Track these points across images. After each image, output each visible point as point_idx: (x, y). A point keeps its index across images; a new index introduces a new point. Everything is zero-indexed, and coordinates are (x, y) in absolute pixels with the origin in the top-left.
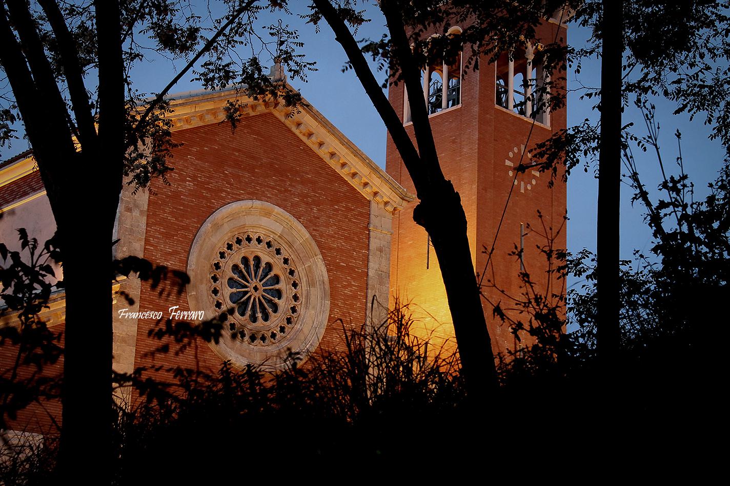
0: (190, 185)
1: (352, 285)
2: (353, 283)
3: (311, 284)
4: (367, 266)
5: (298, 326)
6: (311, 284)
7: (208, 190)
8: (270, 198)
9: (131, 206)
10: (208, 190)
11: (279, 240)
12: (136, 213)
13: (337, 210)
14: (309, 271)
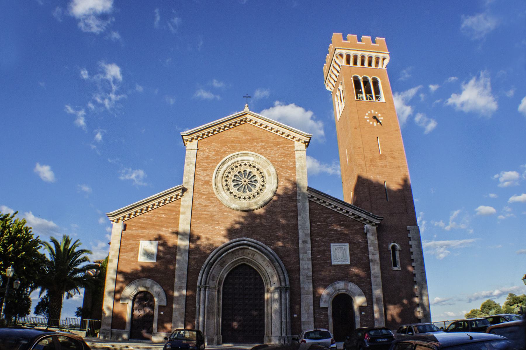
0: (213, 153)
1: (288, 172)
3: (270, 175)
4: (295, 164)
5: (265, 191)
6: (270, 175)
7: (221, 153)
8: (248, 150)
9: (189, 163)
10: (221, 153)
11: (254, 163)
12: (191, 165)
13: (279, 148)
14: (268, 171)
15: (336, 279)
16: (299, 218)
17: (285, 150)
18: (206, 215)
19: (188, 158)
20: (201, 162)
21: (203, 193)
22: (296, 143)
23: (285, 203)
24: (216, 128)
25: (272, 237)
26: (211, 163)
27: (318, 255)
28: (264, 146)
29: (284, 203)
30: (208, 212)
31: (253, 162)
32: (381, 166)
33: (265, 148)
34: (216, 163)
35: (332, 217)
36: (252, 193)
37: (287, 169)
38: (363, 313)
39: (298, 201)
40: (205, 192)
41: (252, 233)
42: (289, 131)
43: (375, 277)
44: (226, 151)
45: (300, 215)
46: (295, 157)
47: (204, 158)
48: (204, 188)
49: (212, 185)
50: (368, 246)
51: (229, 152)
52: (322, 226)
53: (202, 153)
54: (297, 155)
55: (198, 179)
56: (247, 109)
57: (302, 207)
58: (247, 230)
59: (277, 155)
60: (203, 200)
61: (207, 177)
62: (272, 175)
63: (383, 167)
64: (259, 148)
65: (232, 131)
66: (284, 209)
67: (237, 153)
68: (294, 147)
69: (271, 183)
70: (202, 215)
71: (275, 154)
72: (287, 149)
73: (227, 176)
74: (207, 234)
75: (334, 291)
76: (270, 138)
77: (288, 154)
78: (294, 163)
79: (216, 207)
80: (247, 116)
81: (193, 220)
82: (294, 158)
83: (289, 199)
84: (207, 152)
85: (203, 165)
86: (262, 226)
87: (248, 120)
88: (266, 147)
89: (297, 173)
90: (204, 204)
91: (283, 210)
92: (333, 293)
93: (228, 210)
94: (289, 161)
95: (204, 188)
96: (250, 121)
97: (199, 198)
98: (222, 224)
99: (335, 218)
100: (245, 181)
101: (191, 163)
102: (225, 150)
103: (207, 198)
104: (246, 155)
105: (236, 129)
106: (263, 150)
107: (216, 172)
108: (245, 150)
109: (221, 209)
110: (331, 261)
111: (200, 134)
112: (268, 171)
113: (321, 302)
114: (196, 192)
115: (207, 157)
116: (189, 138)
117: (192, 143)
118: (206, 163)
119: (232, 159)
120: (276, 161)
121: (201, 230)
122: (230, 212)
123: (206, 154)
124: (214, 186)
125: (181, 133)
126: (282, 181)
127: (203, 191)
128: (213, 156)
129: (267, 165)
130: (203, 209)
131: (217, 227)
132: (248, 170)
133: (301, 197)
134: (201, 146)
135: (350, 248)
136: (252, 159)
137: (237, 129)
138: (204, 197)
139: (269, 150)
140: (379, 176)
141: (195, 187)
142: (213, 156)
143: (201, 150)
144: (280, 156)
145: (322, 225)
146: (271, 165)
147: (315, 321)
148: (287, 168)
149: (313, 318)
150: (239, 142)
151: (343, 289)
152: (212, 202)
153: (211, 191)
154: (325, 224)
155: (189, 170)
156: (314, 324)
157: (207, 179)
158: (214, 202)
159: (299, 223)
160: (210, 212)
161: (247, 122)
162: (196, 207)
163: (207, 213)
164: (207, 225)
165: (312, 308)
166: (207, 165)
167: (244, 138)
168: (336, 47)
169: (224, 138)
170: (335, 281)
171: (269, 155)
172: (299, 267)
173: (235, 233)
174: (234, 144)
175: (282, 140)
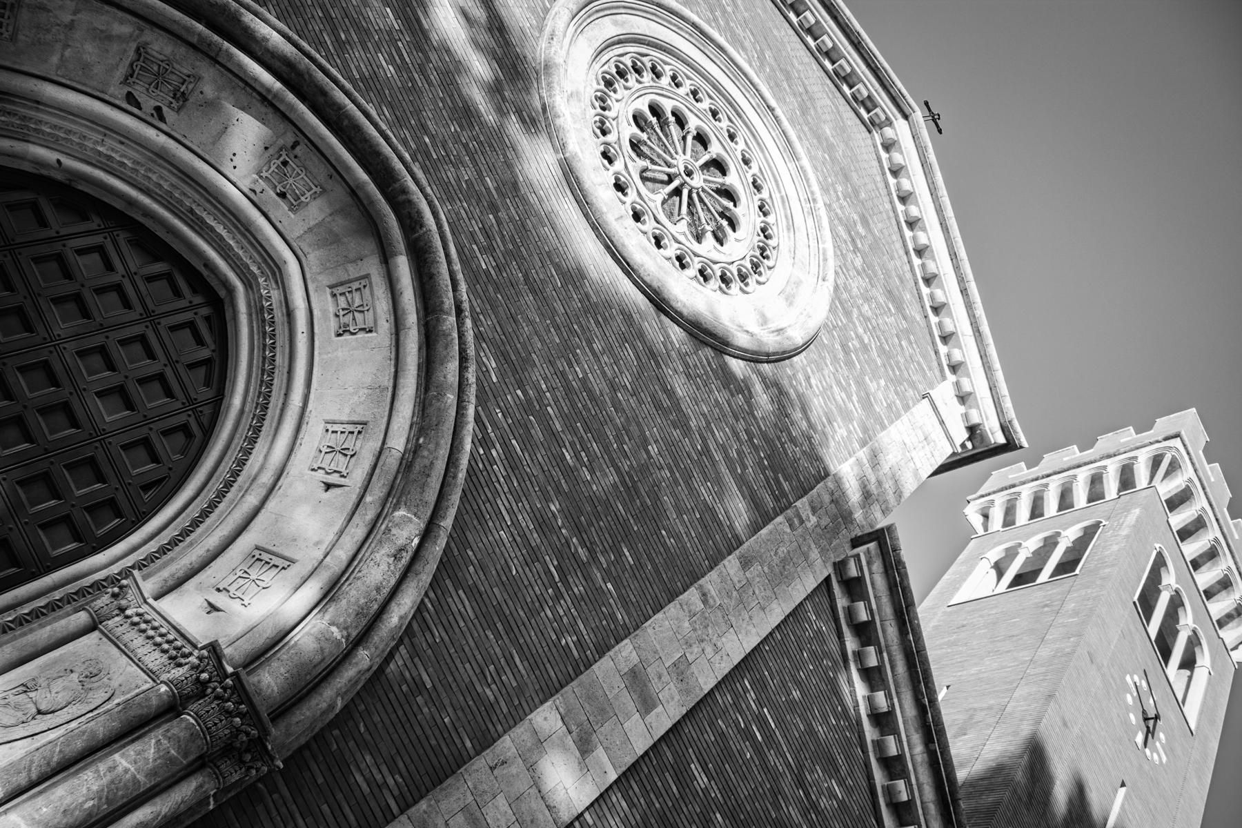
1: (849, 397)
7: (727, 23)
17: (901, 345)
25: (537, 433)
31: (776, 196)
52: (772, 757)
80: (901, 124)
86: (557, 328)
87: (888, 132)
99: (841, 803)
129: (814, 269)
133: (814, 519)
154: (789, 766)
159: (710, 581)
168: (1183, 433)
172: (461, 760)
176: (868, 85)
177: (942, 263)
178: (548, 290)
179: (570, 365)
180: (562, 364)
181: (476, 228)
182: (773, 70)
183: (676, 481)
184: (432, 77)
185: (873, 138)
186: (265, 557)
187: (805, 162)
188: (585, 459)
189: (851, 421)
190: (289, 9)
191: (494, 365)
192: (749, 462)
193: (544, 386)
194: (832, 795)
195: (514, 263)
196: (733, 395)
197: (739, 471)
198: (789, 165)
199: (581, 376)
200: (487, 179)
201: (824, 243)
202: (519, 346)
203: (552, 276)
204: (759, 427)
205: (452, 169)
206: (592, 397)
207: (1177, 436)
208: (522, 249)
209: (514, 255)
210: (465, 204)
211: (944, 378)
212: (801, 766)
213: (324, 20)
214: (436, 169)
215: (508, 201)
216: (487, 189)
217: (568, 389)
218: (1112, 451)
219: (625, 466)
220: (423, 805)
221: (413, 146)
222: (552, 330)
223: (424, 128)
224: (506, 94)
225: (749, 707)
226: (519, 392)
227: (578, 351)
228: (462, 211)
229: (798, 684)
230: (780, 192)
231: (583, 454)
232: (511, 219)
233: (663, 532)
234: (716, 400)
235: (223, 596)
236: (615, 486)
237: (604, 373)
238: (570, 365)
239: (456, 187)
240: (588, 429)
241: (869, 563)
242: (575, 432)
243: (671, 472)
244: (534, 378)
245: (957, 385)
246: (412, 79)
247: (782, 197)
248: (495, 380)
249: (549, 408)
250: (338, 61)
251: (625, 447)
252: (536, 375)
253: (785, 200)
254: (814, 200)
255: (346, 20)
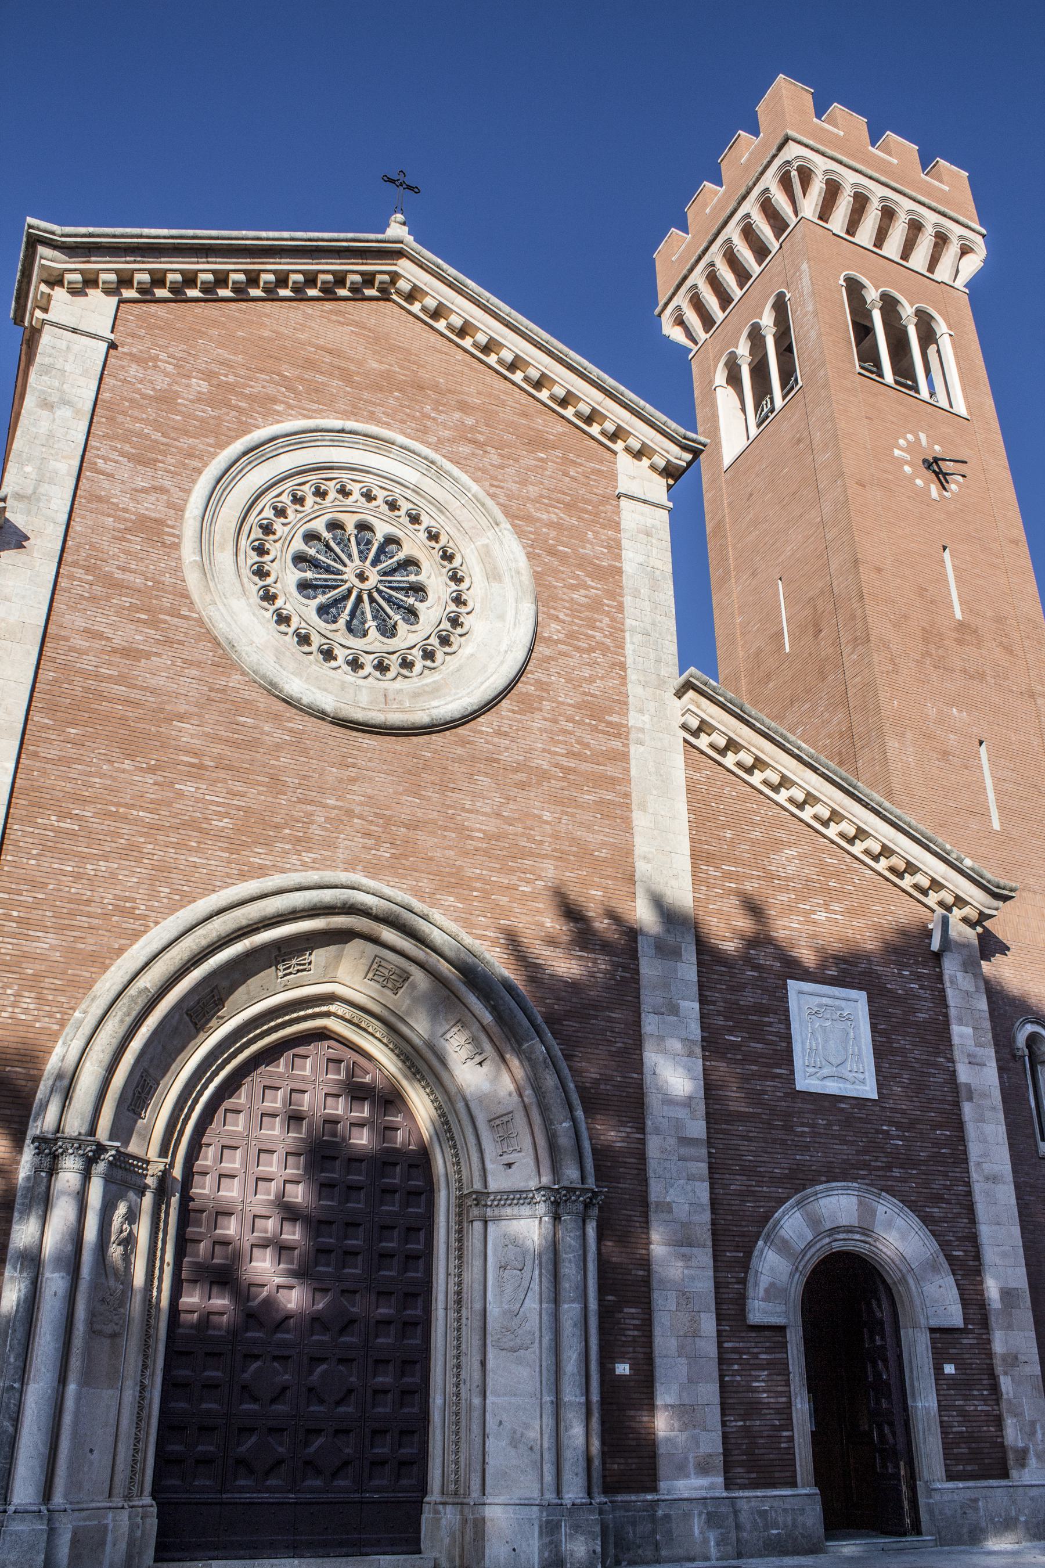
1: (587, 587)
2: (590, 583)
3: (493, 575)
4: (619, 557)
6: (493, 575)
7: (246, 397)
9: (54, 399)
10: (246, 397)
13: (541, 460)
14: (485, 555)
15: (819, 1173)
16: (640, 820)
17: (573, 478)
18: (127, 702)
19: (48, 369)
20: (124, 413)
21: (118, 575)
22: (624, 461)
23: (571, 733)
24: (236, 270)
25: (503, 900)
26: (186, 433)
27: (731, 1031)
28: (473, 429)
29: (564, 731)
30: (144, 689)
31: (409, 494)
32: (964, 671)
33: (474, 442)
34: (211, 441)
35: (790, 845)
36: (394, 643)
37: (580, 566)
38: (949, 1369)
39: (633, 736)
40: (129, 577)
41: (394, 856)
42: (599, 396)
43: (987, 1179)
44: (274, 400)
45: (643, 807)
46: (619, 523)
47: (144, 396)
48: (127, 553)
49: (176, 546)
50: (946, 1016)
51: (290, 407)
53: (134, 371)
54: (630, 515)
55: (99, 499)
56: (397, 230)
57: (652, 770)
58: (368, 835)
59: (533, 491)
60: (118, 614)
61: (152, 498)
62: (507, 579)
63: (972, 677)
64: (447, 433)
65: (310, 311)
66: (564, 762)
67: (338, 424)
68: (613, 476)
69: (501, 617)
70: (101, 696)
71: (524, 482)
72: (581, 478)
73: (267, 529)
74: (124, 818)
75: (810, 1237)
76: (503, 404)
77: (588, 502)
78: (615, 548)
79: (194, 672)
80: (404, 266)
81: (36, 717)
82: (616, 526)
83: (591, 717)
84: (167, 374)
85: (139, 434)
86: (445, 828)
87: (403, 285)
88: (481, 438)
89: (628, 600)
90: (118, 641)
91: (557, 765)
92: (810, 1245)
93: (263, 701)
94: (590, 535)
95: (127, 553)
96: (412, 296)
97: (93, 599)
98: (222, 774)
99: (801, 857)
100: (362, 577)
101: (65, 402)
102: (271, 390)
103: (139, 610)
104: (382, 444)
105: (330, 312)
106: (465, 449)
107: (213, 482)
108: (372, 418)
109: (222, 691)
110: (792, 1072)
111: (142, 270)
112: (485, 555)
113: (750, 1292)
114: (75, 564)
115: (166, 399)
116: (73, 268)
117: (80, 300)
118: (157, 425)
119: (300, 446)
120: (529, 519)
121: (88, 785)
122: (277, 717)
123: (162, 383)
124: (188, 553)
125: (30, 220)
126: (557, 619)
127: (119, 568)
128: (199, 400)
129: (484, 522)
130: (109, 664)
131: (188, 788)
132: (382, 529)
133: (646, 718)
134: (133, 336)
135: (872, 1015)
136: (409, 475)
137: (338, 313)
138: (126, 601)
139: (496, 459)
140: (960, 711)
141: (71, 533)
142: (199, 400)
143: (131, 355)
144: (549, 498)
145: (750, 877)
146: (506, 525)
147: (725, 1408)
148: (583, 562)
149: (715, 1387)
150: (346, 377)
151: (850, 1230)
152: (168, 642)
153: (167, 579)
155: (51, 435)
156: (724, 1424)
157: (151, 506)
158: (181, 643)
160: (154, 691)
161: (394, 297)
162: (72, 649)
163: (135, 695)
164: (128, 765)
165: (708, 1324)
166: (157, 436)
167: (375, 365)
169: (266, 334)
170: (815, 1182)
171: (495, 478)
172: (640, 1086)
173: (298, 840)
174: (320, 378)
175: (561, 429)
176: (354, 269)
177: (540, 362)
178: (419, 814)
179: (471, 838)
180: (471, 844)
181: (361, 840)
182: (301, 379)
183: (573, 815)
184: (240, 789)
185: (394, 302)
186: (498, 1122)
187: (401, 439)
188: (531, 876)
189: (602, 604)
190: (165, 874)
191: (452, 899)
192: (587, 738)
193: (478, 871)
194: (789, 860)
195: (393, 828)
196: (540, 710)
197: (589, 753)
198: (391, 456)
199: (482, 835)
200: (328, 801)
201: (469, 491)
202: (447, 870)
203: (410, 802)
204: (570, 705)
205: (314, 826)
206: (498, 837)
207: (787, 139)
208: (385, 812)
209: (388, 821)
210: (342, 836)
211: (615, 453)
212: (764, 869)
213: (178, 851)
214: (309, 840)
215: (348, 796)
216: (335, 808)
217: (487, 853)
218: (742, 191)
219: (547, 848)
220: (649, 1123)
221: (289, 846)
222: (446, 833)
223: (277, 827)
224: (266, 728)
225: (716, 878)
226: (475, 894)
227: (466, 824)
228: (346, 842)
229: (724, 827)
230: (408, 488)
231: (528, 876)
232: (361, 804)
233: (596, 853)
234: (540, 729)
235: (505, 1156)
236: (556, 867)
237: (486, 814)
238: (471, 838)
239: (327, 834)
240: (514, 858)
241: (698, 707)
242: (512, 871)
243: (566, 813)
244: (470, 875)
245: (627, 449)
246: (238, 808)
247: (413, 490)
248: (460, 906)
249: (493, 879)
250: (213, 862)
251: (537, 838)
252: (470, 872)
253: (417, 490)
254: (432, 462)
255: (180, 831)
